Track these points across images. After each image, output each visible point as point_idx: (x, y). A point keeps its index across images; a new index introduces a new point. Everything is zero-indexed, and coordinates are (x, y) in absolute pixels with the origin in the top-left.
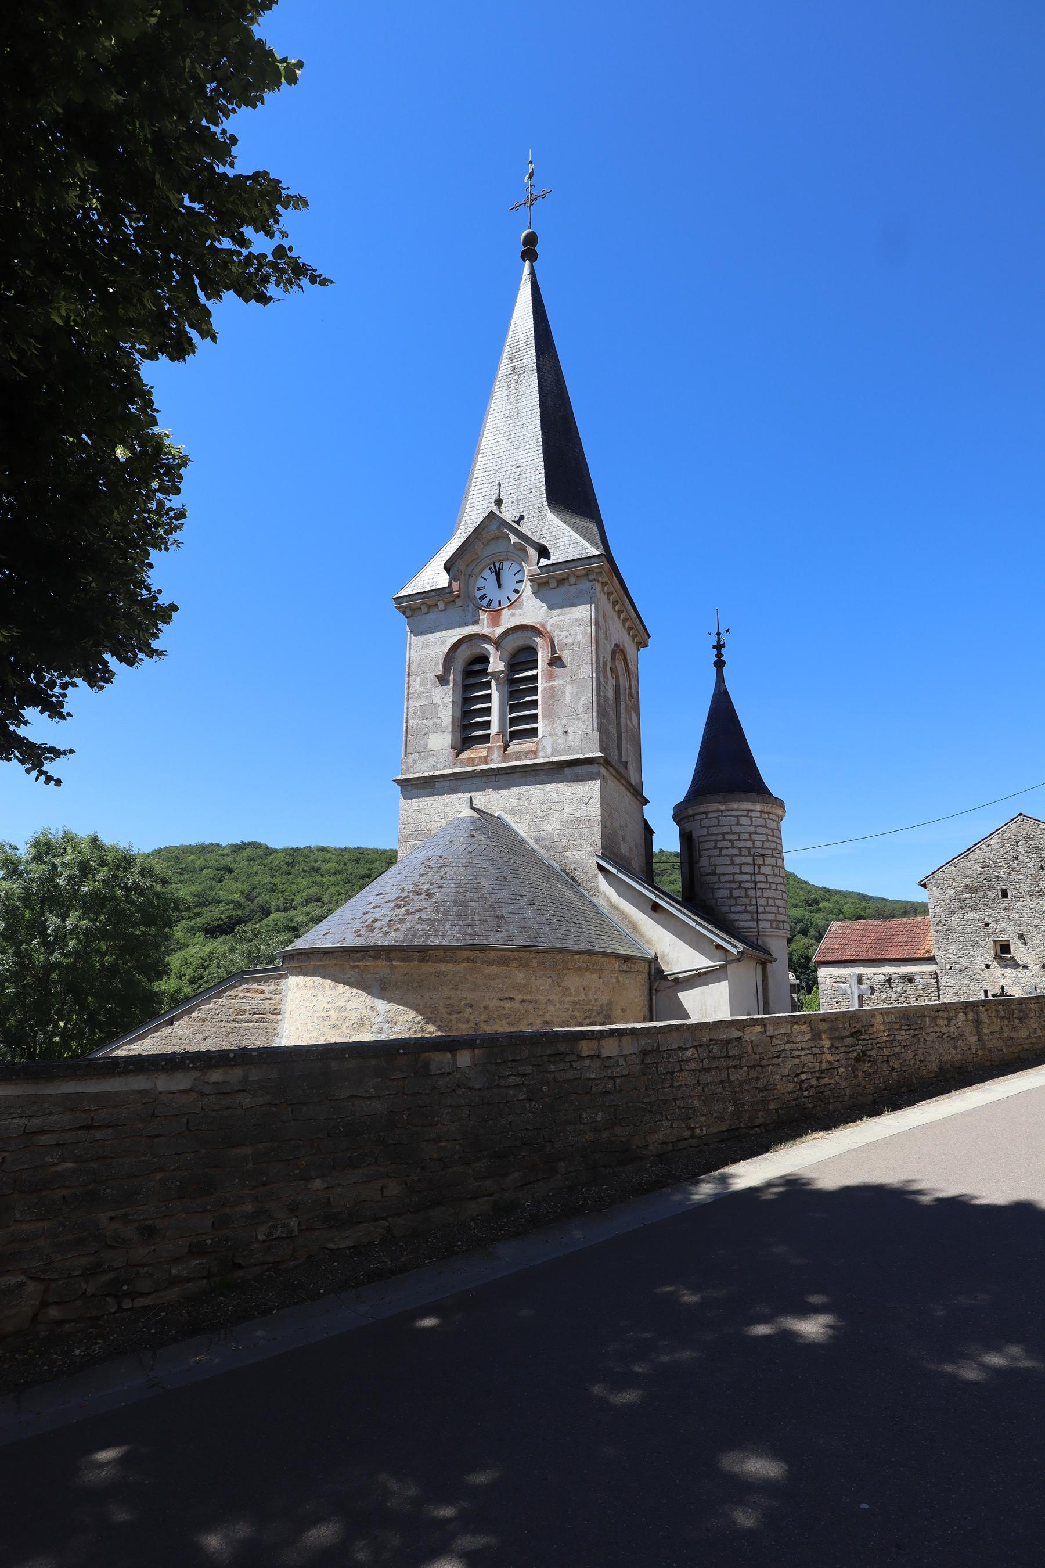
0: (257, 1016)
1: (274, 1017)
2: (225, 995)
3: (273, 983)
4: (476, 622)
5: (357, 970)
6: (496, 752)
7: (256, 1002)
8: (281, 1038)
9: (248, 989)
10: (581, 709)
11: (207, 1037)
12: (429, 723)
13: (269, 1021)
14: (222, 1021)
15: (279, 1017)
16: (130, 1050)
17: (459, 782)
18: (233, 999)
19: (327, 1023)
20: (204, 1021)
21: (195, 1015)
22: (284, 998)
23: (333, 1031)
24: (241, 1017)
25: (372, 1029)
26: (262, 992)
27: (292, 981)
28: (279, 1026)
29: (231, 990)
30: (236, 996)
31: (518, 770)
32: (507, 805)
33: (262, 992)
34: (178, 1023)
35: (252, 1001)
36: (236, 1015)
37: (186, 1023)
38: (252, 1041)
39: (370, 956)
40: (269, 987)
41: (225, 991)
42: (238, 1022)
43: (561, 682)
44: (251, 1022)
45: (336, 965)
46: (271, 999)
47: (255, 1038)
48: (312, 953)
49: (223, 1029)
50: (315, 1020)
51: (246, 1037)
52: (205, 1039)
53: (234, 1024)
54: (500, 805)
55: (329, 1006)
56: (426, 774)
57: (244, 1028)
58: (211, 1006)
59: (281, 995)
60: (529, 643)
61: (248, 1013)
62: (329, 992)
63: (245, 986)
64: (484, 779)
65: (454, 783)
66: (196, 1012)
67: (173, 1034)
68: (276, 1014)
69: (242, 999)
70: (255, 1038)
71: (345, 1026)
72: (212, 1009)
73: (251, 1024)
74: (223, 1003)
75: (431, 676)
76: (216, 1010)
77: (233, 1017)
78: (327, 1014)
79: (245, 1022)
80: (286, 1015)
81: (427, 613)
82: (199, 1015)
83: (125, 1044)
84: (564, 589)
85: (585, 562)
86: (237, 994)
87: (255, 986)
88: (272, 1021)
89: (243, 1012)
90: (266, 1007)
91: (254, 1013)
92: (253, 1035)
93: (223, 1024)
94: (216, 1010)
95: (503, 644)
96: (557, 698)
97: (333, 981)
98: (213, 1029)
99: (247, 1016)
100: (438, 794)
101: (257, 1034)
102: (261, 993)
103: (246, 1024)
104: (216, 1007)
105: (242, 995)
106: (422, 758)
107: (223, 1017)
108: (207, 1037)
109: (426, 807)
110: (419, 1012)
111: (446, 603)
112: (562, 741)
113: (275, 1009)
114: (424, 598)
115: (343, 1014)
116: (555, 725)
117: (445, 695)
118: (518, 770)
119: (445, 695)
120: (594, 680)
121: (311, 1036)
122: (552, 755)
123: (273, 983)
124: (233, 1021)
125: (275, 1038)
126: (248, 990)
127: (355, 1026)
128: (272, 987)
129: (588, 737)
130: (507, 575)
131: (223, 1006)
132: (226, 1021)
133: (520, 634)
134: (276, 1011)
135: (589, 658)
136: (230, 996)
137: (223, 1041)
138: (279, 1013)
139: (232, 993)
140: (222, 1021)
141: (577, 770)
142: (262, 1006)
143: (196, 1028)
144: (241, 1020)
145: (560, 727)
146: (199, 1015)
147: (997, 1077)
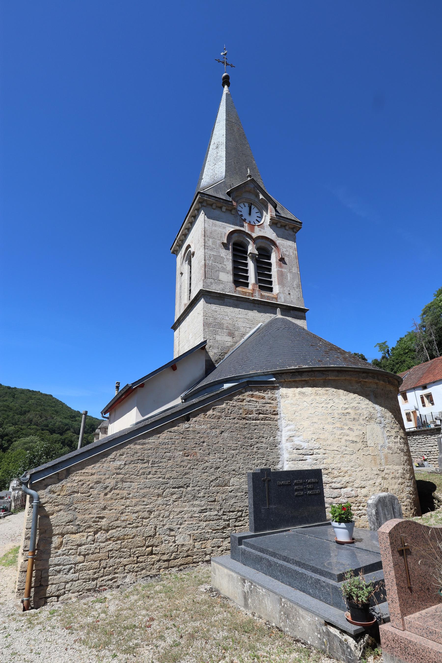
0: (261, 416)
1: (273, 416)
2: (235, 398)
3: (269, 392)
4: (243, 226)
5: (360, 384)
6: (257, 292)
7: (260, 405)
8: (281, 432)
9: (252, 395)
10: (295, 286)
11: (223, 432)
12: (220, 266)
13: (271, 419)
14: (235, 418)
15: (278, 417)
16: (145, 444)
17: (239, 302)
18: (241, 402)
19: (348, 417)
20: (219, 418)
21: (210, 412)
22: (279, 403)
23: (354, 422)
24: (250, 416)
25: (377, 421)
26: (263, 398)
27: (283, 391)
28: (279, 422)
29: (240, 395)
30: (244, 400)
31: (270, 305)
32: (265, 321)
33: (263, 398)
34: (195, 419)
35: (257, 405)
36: (246, 414)
37: (202, 419)
38: (261, 434)
39: (370, 376)
40: (268, 395)
41: (235, 395)
42: (248, 420)
43: (285, 270)
44: (258, 420)
45: (345, 379)
46: (270, 403)
47: (262, 432)
48: (283, 373)
49: (237, 425)
50: (336, 416)
51: (256, 431)
52: (221, 433)
53: (244, 421)
54: (261, 320)
55: (346, 406)
56: (218, 292)
57: (254, 425)
58: (224, 406)
59: (276, 401)
60: (267, 246)
61: (254, 413)
62: (344, 398)
63: (250, 393)
64: (252, 305)
65: (236, 302)
66: (211, 411)
67: (191, 429)
68: (275, 414)
69: (249, 402)
70: (262, 432)
71: (361, 418)
72: (225, 409)
73: (258, 422)
74: (234, 405)
75: (219, 242)
76: (229, 409)
77: (244, 416)
78: (346, 411)
79: (253, 420)
80: (282, 415)
81: (214, 209)
82: (214, 413)
83: (139, 438)
84: (283, 229)
85: (295, 223)
86: (244, 398)
87: (257, 393)
88: (273, 420)
89: (251, 412)
90: (268, 408)
91: (260, 413)
92: (261, 430)
93: (236, 421)
94: (229, 409)
95: (257, 241)
96: (284, 277)
97: (345, 390)
98: (228, 425)
99: (254, 415)
100: (227, 305)
101: (264, 429)
102: (263, 398)
103: (254, 421)
104: (228, 407)
105: (248, 399)
106: (216, 283)
107: (235, 415)
108: (223, 432)
109: (220, 310)
110: (393, 414)
111: (226, 209)
112: (288, 297)
113: (274, 411)
114: (217, 200)
115: (358, 411)
116: (284, 289)
117: (228, 254)
118: (270, 305)
119: (228, 254)
120: (299, 275)
121: (334, 426)
122: (284, 302)
123: (269, 392)
124: (244, 418)
125: (277, 432)
126: (252, 396)
127: (367, 419)
128: (270, 395)
129: (300, 299)
130: (254, 210)
131: (234, 406)
132: (238, 419)
133: (264, 241)
134: (275, 413)
135: (296, 265)
136: (239, 399)
137: (237, 434)
138: (277, 414)
139: (240, 397)
140: (235, 418)
141: (296, 313)
142: (265, 408)
143: (212, 424)
144: (250, 418)
145: (287, 291)
146: (214, 413)
147: (306, 470)
